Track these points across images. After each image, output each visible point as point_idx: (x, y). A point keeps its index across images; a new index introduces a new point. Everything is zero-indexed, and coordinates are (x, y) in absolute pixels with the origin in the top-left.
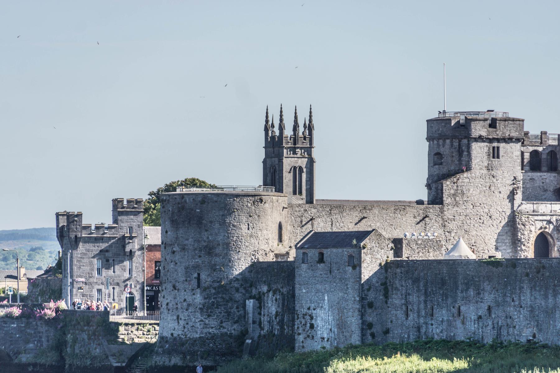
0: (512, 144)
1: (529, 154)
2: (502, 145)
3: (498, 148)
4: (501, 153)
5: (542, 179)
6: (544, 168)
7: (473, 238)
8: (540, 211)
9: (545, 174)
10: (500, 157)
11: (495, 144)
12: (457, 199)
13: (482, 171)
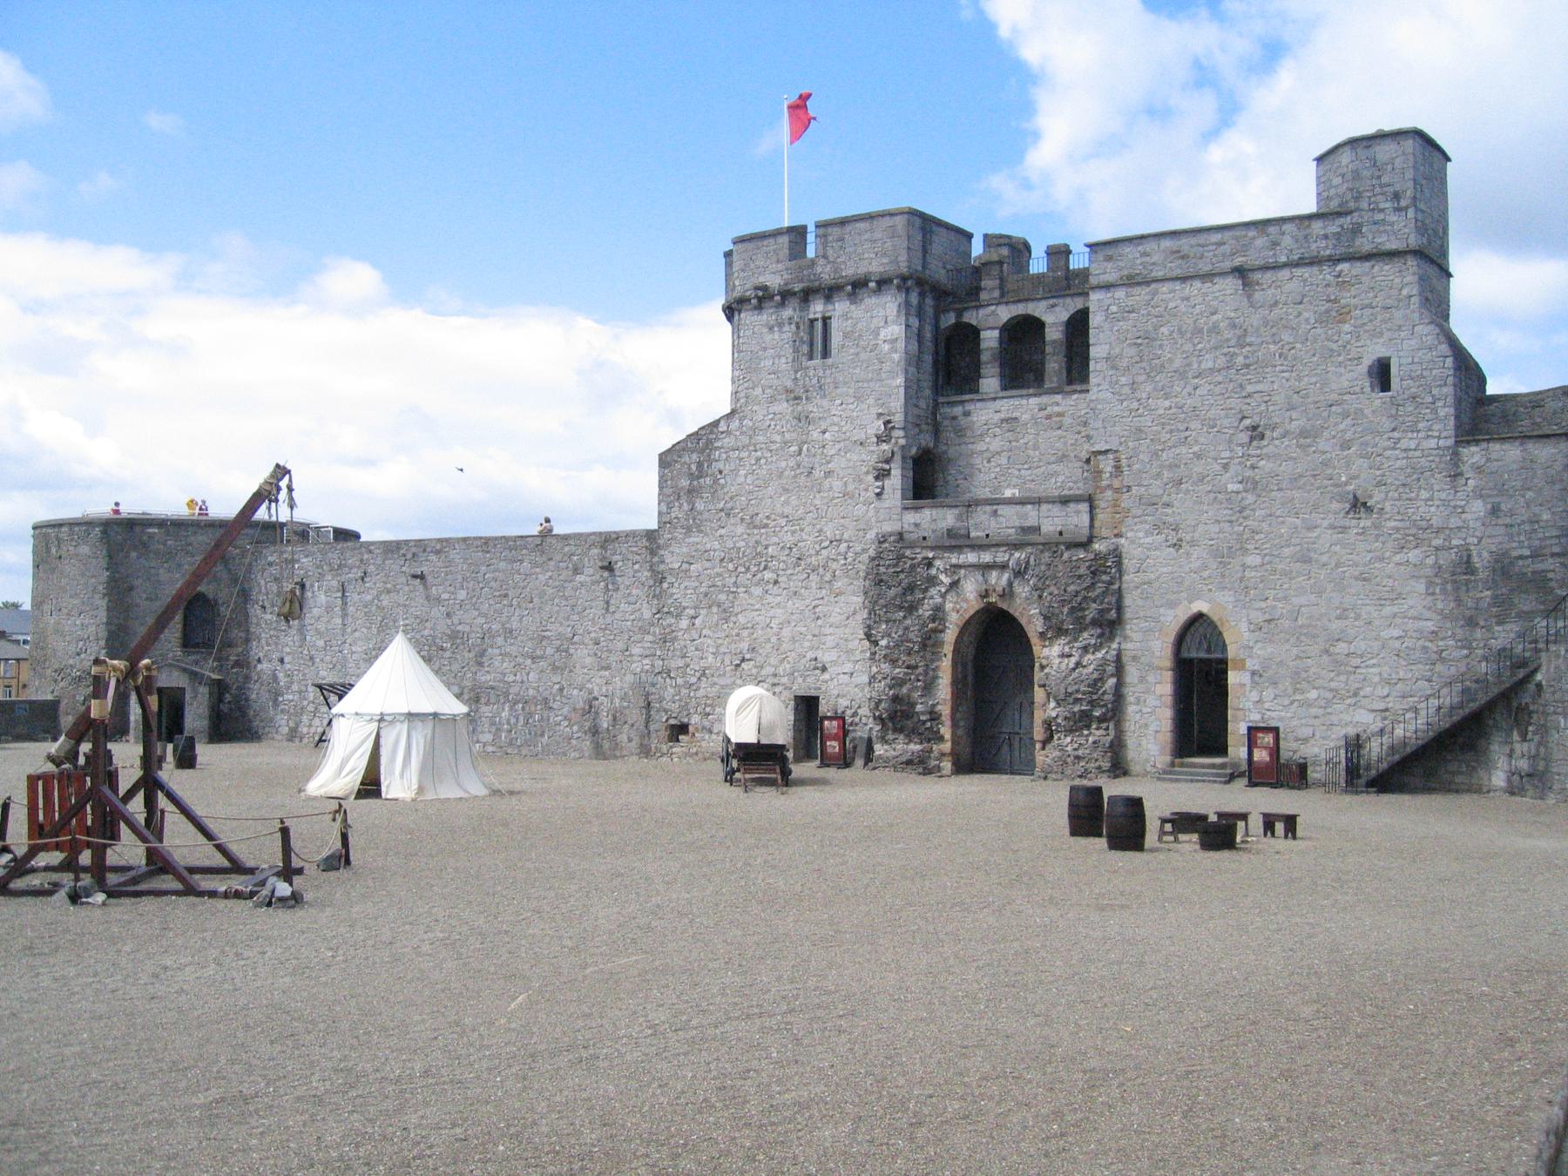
0: (871, 301)
1: (996, 333)
2: (840, 307)
3: (826, 320)
4: (836, 338)
5: (1049, 417)
6: (1051, 380)
7: (745, 633)
8: (973, 534)
9: (1058, 398)
10: (834, 352)
11: (817, 308)
12: (700, 505)
13: (776, 408)
